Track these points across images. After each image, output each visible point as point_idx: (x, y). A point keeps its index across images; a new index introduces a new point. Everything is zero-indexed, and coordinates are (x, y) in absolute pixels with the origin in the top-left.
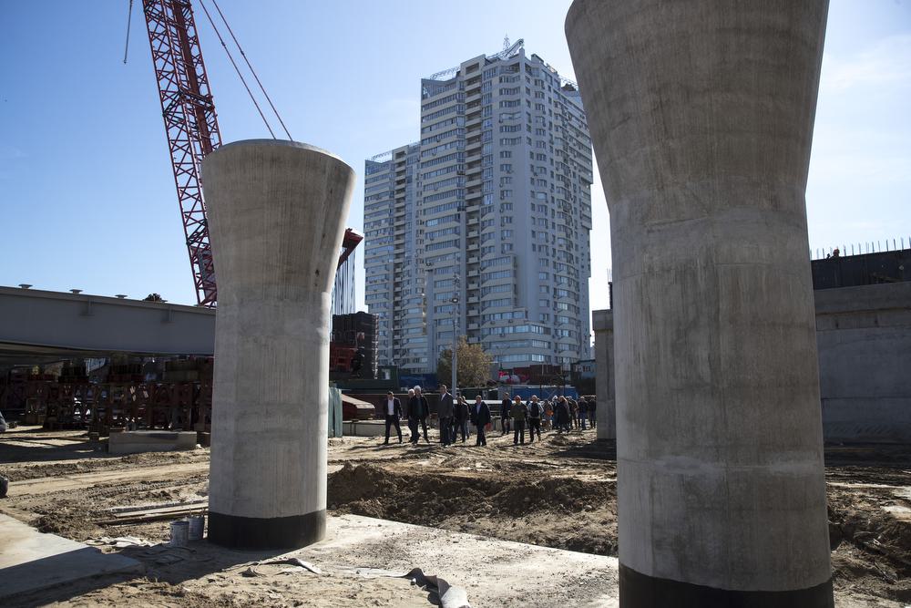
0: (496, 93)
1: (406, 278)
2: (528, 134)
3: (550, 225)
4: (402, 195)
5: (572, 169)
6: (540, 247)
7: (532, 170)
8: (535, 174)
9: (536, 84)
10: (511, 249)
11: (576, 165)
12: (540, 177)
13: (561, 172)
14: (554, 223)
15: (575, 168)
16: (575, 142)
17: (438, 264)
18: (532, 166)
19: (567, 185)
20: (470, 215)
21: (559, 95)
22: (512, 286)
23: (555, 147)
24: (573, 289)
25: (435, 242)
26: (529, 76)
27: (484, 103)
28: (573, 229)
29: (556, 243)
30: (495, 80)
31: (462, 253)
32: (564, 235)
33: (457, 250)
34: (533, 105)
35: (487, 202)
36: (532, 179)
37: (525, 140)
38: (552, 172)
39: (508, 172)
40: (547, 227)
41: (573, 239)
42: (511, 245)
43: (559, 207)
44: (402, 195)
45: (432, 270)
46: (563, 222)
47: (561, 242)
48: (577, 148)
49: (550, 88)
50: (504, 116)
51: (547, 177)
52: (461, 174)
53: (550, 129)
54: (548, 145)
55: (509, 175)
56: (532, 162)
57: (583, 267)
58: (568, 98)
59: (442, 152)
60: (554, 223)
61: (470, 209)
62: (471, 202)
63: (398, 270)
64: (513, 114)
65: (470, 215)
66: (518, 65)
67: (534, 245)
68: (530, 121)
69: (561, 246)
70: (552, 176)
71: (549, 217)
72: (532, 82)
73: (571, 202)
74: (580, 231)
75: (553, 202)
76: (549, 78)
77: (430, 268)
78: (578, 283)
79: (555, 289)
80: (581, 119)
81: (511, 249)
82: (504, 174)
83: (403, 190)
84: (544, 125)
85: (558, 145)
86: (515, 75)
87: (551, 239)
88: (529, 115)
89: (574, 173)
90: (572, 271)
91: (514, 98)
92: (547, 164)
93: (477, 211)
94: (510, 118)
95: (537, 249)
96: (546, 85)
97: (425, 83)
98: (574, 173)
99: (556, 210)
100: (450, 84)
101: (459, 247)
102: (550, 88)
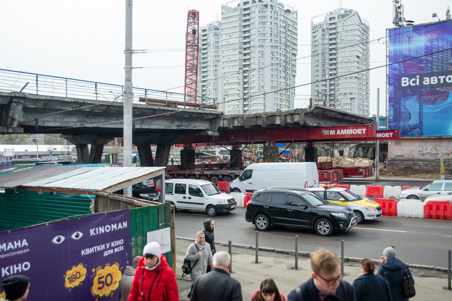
0: (257, 18)
1: (209, 93)
2: (271, 38)
3: (279, 77)
4: (205, 51)
5: (289, 50)
6: (274, 87)
7: (272, 53)
8: (273, 55)
9: (274, 14)
10: (263, 88)
11: (290, 48)
12: (276, 56)
13: (284, 53)
14: (280, 76)
15: (290, 50)
16: (290, 37)
17: (229, 92)
18: (272, 52)
19: (286, 59)
20: (245, 72)
21: (284, 16)
22: (263, 104)
23: (282, 42)
24: (287, 104)
25: (228, 82)
26: (271, 10)
27: (252, 21)
28: (288, 78)
29: (281, 85)
30: (257, 12)
31: (241, 88)
32: (284, 81)
33: (239, 87)
34: (273, 24)
35: (253, 66)
36: (272, 58)
37: (269, 40)
38: (280, 54)
39: (262, 55)
40: (278, 79)
41: (288, 82)
42: (263, 86)
43: (283, 69)
44: (205, 51)
45: (227, 95)
46: (284, 75)
47: (283, 84)
48: (291, 40)
49: (280, 14)
50: (260, 29)
51: (278, 56)
52: (240, 53)
53: (280, 34)
54: (279, 41)
55: (262, 56)
56: (272, 50)
57: (292, 94)
58: (288, 17)
59: (231, 41)
60: (280, 76)
61: (245, 69)
62: (245, 66)
63: (204, 89)
64: (264, 28)
65: (245, 72)
66: (267, 5)
67: (272, 86)
68: (272, 32)
69: (283, 86)
70: (280, 56)
71: (278, 74)
72: (273, 13)
73: (288, 66)
74: (292, 77)
75: (280, 67)
76: (280, 9)
77: (226, 94)
78: (290, 101)
79: (280, 105)
80: (293, 26)
81: (263, 88)
82: (260, 55)
83: (206, 49)
84: (278, 33)
85: (283, 41)
86: (266, 10)
87: (279, 83)
88: (271, 28)
89: (289, 52)
90: (287, 96)
91: (266, 20)
92: (278, 51)
93: (248, 71)
94: (263, 30)
95: (273, 87)
96: (279, 14)
97: (222, 5)
98: (289, 52)
99: (282, 70)
100: (235, 10)
101: (240, 85)
102: (280, 14)
